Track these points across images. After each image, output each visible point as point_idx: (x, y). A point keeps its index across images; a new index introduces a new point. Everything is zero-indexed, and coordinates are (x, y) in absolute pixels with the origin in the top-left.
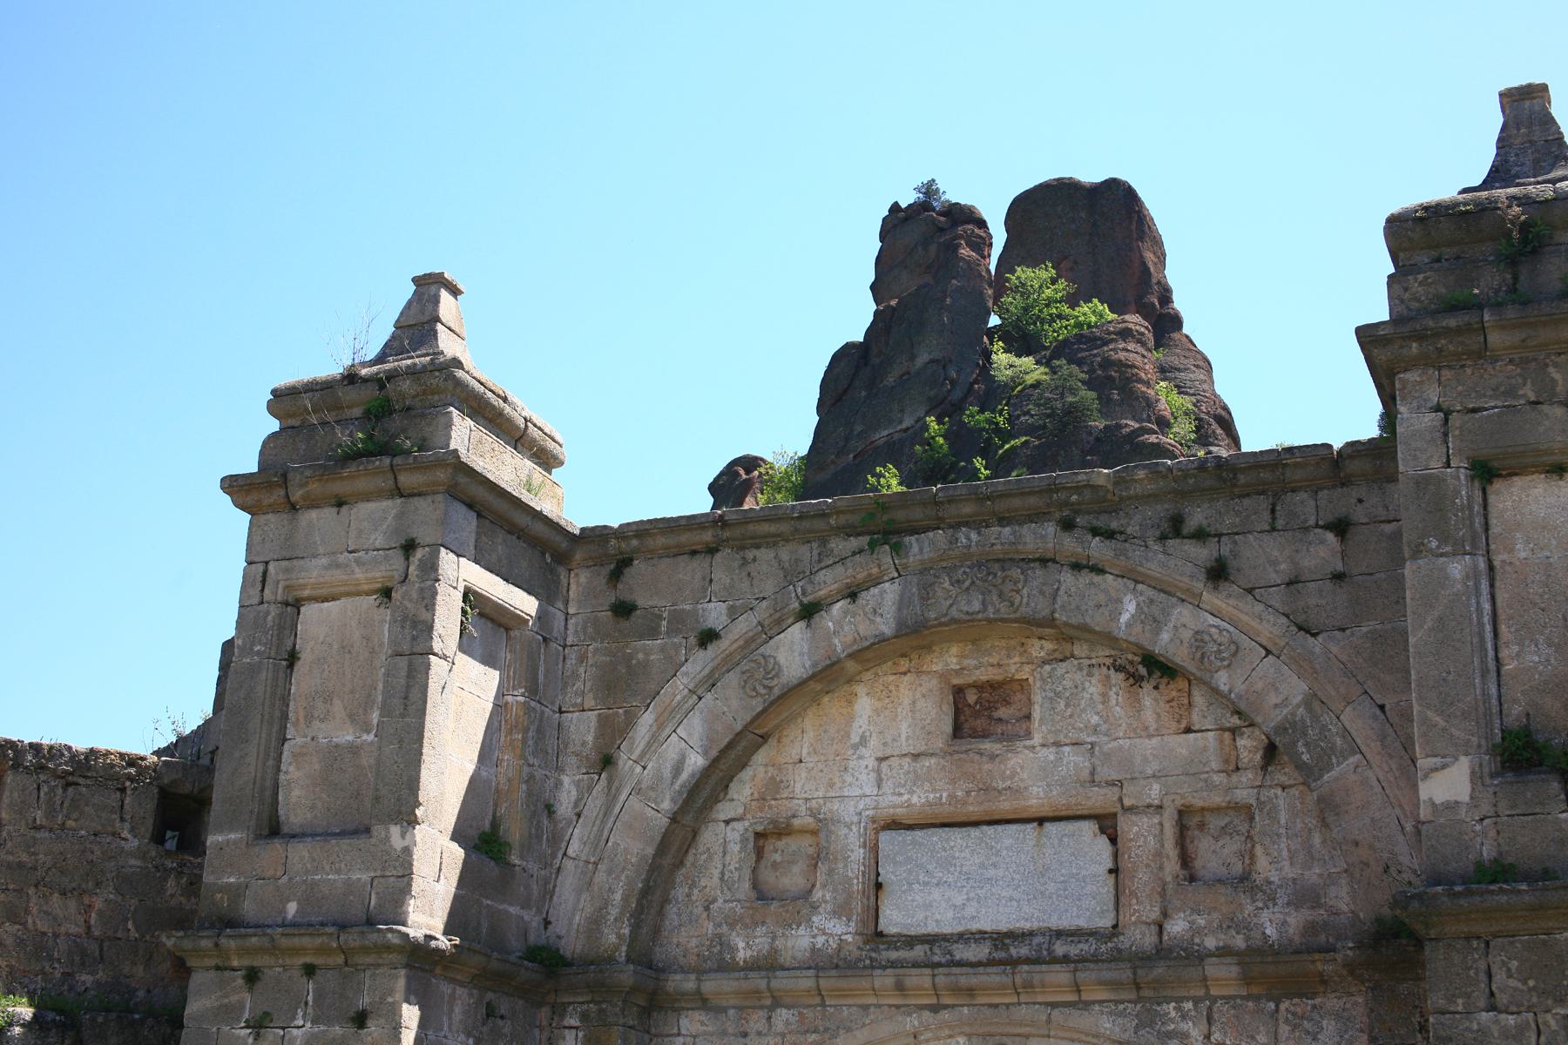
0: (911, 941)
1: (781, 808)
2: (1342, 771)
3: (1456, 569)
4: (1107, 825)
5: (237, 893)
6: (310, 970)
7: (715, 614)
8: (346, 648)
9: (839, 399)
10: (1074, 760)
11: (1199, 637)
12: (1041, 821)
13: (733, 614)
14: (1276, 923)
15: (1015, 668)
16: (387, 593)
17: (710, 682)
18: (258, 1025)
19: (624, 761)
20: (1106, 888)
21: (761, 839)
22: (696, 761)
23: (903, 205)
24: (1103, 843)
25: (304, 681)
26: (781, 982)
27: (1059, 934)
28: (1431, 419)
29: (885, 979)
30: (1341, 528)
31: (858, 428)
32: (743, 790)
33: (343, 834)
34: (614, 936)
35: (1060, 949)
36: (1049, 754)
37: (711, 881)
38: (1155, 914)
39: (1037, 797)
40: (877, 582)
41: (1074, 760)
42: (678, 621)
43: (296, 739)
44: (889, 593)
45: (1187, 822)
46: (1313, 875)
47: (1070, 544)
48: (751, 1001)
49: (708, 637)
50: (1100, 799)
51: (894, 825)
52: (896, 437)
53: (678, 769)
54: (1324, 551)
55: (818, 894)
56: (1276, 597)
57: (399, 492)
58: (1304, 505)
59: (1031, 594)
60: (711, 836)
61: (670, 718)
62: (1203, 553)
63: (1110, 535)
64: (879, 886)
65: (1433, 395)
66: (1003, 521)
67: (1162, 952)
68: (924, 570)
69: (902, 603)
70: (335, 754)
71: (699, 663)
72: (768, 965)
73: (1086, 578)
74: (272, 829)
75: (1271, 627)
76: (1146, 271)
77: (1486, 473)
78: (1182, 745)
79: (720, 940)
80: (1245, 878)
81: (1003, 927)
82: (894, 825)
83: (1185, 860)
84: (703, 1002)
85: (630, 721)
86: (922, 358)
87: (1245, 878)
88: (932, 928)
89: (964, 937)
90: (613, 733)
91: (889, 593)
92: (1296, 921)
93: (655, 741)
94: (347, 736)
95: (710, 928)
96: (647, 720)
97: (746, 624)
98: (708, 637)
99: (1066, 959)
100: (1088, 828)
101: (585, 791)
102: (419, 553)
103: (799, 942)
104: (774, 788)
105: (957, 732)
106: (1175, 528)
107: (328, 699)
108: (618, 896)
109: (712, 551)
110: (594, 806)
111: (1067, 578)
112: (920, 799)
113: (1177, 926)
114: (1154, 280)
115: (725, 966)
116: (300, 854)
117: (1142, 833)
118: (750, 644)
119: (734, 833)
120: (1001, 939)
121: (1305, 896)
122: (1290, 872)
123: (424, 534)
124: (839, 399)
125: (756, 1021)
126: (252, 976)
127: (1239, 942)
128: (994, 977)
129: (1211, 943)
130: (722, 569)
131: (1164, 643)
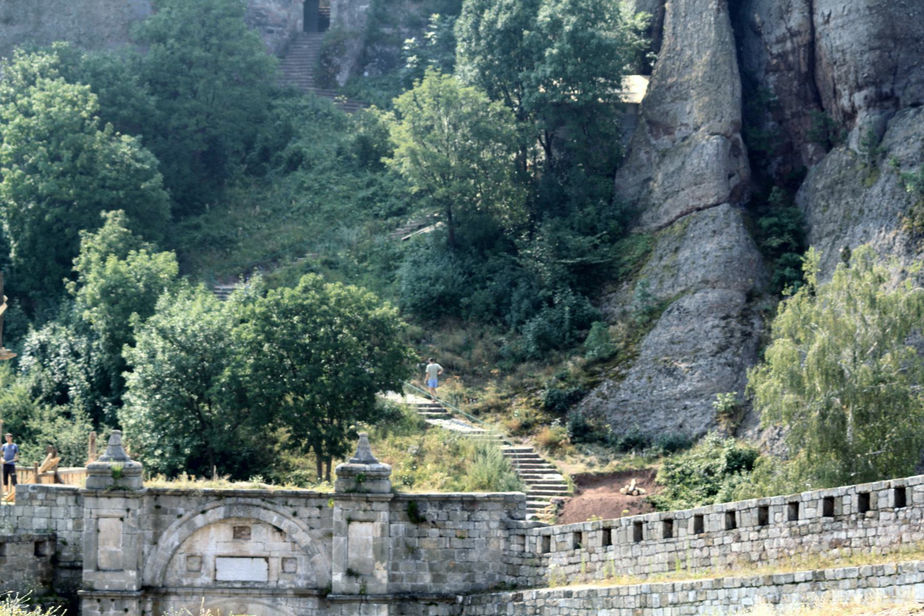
0: (224, 582)
1: (193, 552)
2: (317, 557)
3: (342, 539)
4: (267, 559)
5: (92, 583)
6: (113, 600)
7: (181, 510)
8: (111, 529)
10: (260, 546)
11: (290, 527)
12: (252, 557)
13: (186, 511)
14: (301, 583)
15: (247, 524)
16: (122, 519)
17: (180, 526)
18: (102, 610)
20: (266, 573)
22: (177, 543)
24: (265, 564)
25: (101, 536)
26: (196, 590)
27: (256, 582)
28: (340, 511)
29: (219, 591)
30: (320, 507)
32: (184, 547)
33: (116, 571)
35: (256, 585)
36: (255, 544)
37: (177, 567)
38: (276, 579)
39: (252, 553)
40: (218, 507)
41: (260, 546)
42: (172, 512)
43: (101, 549)
44: (222, 510)
45: (284, 560)
46: (309, 573)
47: (263, 504)
48: (187, 594)
49: (180, 516)
50: (265, 554)
51: (220, 556)
53: (172, 545)
54: (316, 512)
55: (202, 571)
56: (306, 520)
57: (125, 497)
58: (313, 502)
59: (254, 512)
60: (177, 557)
61: (172, 533)
62: (292, 510)
63: (272, 503)
64: (216, 570)
65: (341, 506)
66: (249, 497)
67: (278, 588)
68: (230, 505)
69: (225, 512)
70: (111, 554)
71: (177, 522)
72: (191, 586)
73: (266, 511)
74: (98, 569)
75: (305, 527)
77: (350, 521)
78: (284, 545)
79: (180, 581)
80: (295, 572)
81: (244, 579)
82: (220, 556)
83: (283, 568)
84: (176, 594)
85: (161, 534)
87: (295, 572)
88: (227, 579)
89: (235, 582)
91: (222, 510)
92: (305, 582)
93: (167, 538)
94: (114, 549)
95: (177, 577)
96: (165, 534)
97: (188, 514)
98: (180, 516)
99: (257, 588)
100: (263, 560)
101: (150, 549)
102: (131, 512)
103: (198, 581)
104: (190, 547)
105: (234, 537)
106: (286, 504)
107: (108, 540)
108: (159, 572)
109: (180, 496)
110: (153, 552)
111: (263, 511)
112: (225, 552)
113: (281, 582)
115: (182, 587)
116: (108, 575)
117: (275, 563)
118: (189, 519)
119: (182, 556)
120: (244, 582)
121: (307, 578)
122: (304, 572)
123: (132, 507)
125: (188, 598)
126: (99, 601)
127: (293, 586)
128: (243, 591)
129: (288, 586)
130: (183, 500)
131: (282, 527)
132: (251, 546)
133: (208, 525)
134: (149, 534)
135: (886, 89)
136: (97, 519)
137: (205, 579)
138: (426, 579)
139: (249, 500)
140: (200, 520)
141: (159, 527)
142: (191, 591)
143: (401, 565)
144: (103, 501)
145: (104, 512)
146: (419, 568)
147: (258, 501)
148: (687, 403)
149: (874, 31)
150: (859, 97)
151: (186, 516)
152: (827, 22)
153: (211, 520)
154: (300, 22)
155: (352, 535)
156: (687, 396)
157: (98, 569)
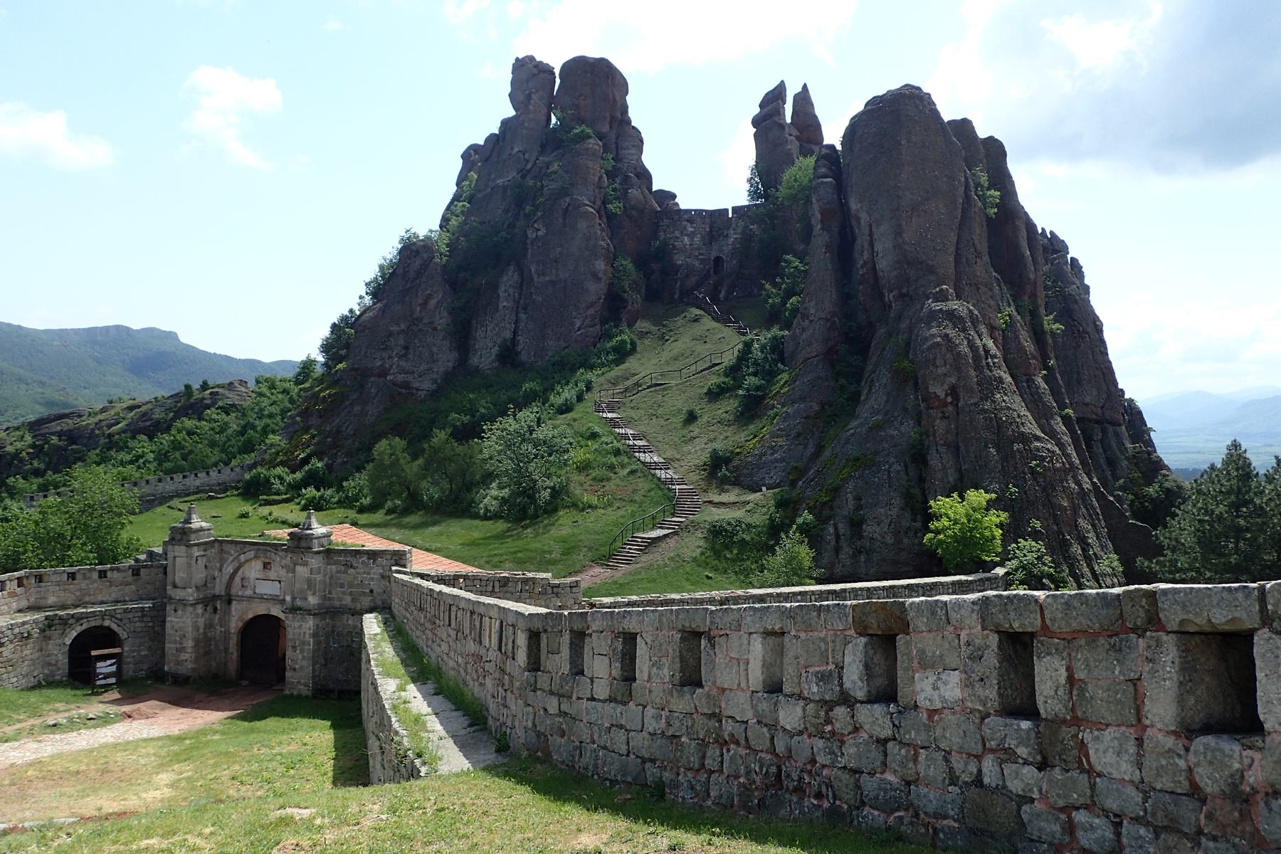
4: (280, 582)
7: (233, 552)
9: (486, 160)
17: (233, 561)
19: (223, 570)
21: (242, 579)
23: (520, 57)
31: (492, 176)
32: (240, 572)
34: (223, 593)
39: (272, 578)
42: (229, 553)
44: (253, 552)
52: (506, 183)
60: (236, 578)
70: (182, 578)
74: (175, 586)
76: (615, 101)
86: (516, 150)
90: (221, 566)
96: (225, 566)
104: (243, 573)
112: (260, 577)
114: (619, 104)
116: (178, 590)
124: (486, 160)
130: (233, 546)
132: (272, 574)
133: (247, 561)
134: (218, 565)
135: (904, 291)
136: (175, 557)
137: (249, 592)
138: (348, 600)
139: (264, 547)
140: (242, 558)
141: (222, 561)
142: (242, 598)
143: (333, 591)
144: (176, 547)
145: (177, 554)
146: (344, 593)
147: (268, 548)
148: (777, 464)
149: (896, 259)
150: (891, 295)
151: (234, 556)
152: (877, 256)
153: (248, 558)
154: (712, 271)
155: (297, 574)
156: (776, 460)
157: (175, 586)
